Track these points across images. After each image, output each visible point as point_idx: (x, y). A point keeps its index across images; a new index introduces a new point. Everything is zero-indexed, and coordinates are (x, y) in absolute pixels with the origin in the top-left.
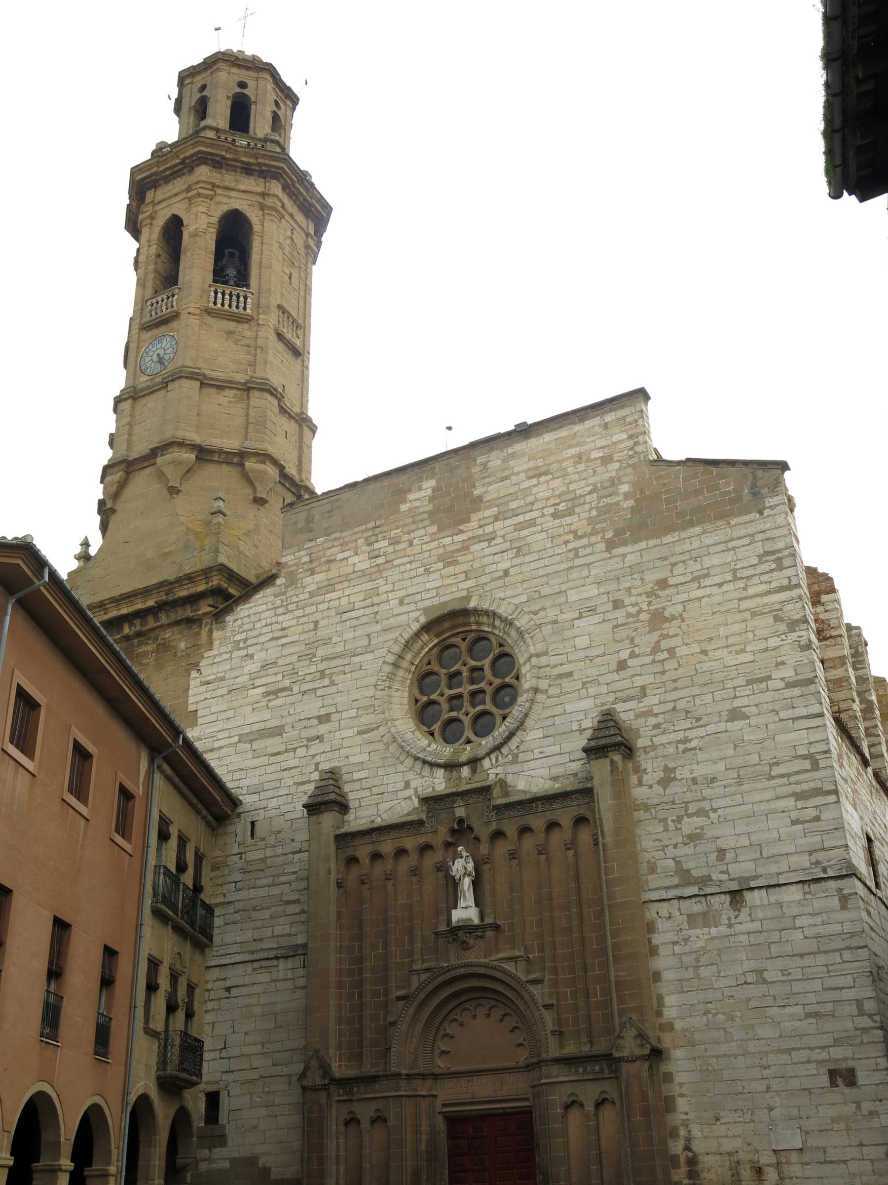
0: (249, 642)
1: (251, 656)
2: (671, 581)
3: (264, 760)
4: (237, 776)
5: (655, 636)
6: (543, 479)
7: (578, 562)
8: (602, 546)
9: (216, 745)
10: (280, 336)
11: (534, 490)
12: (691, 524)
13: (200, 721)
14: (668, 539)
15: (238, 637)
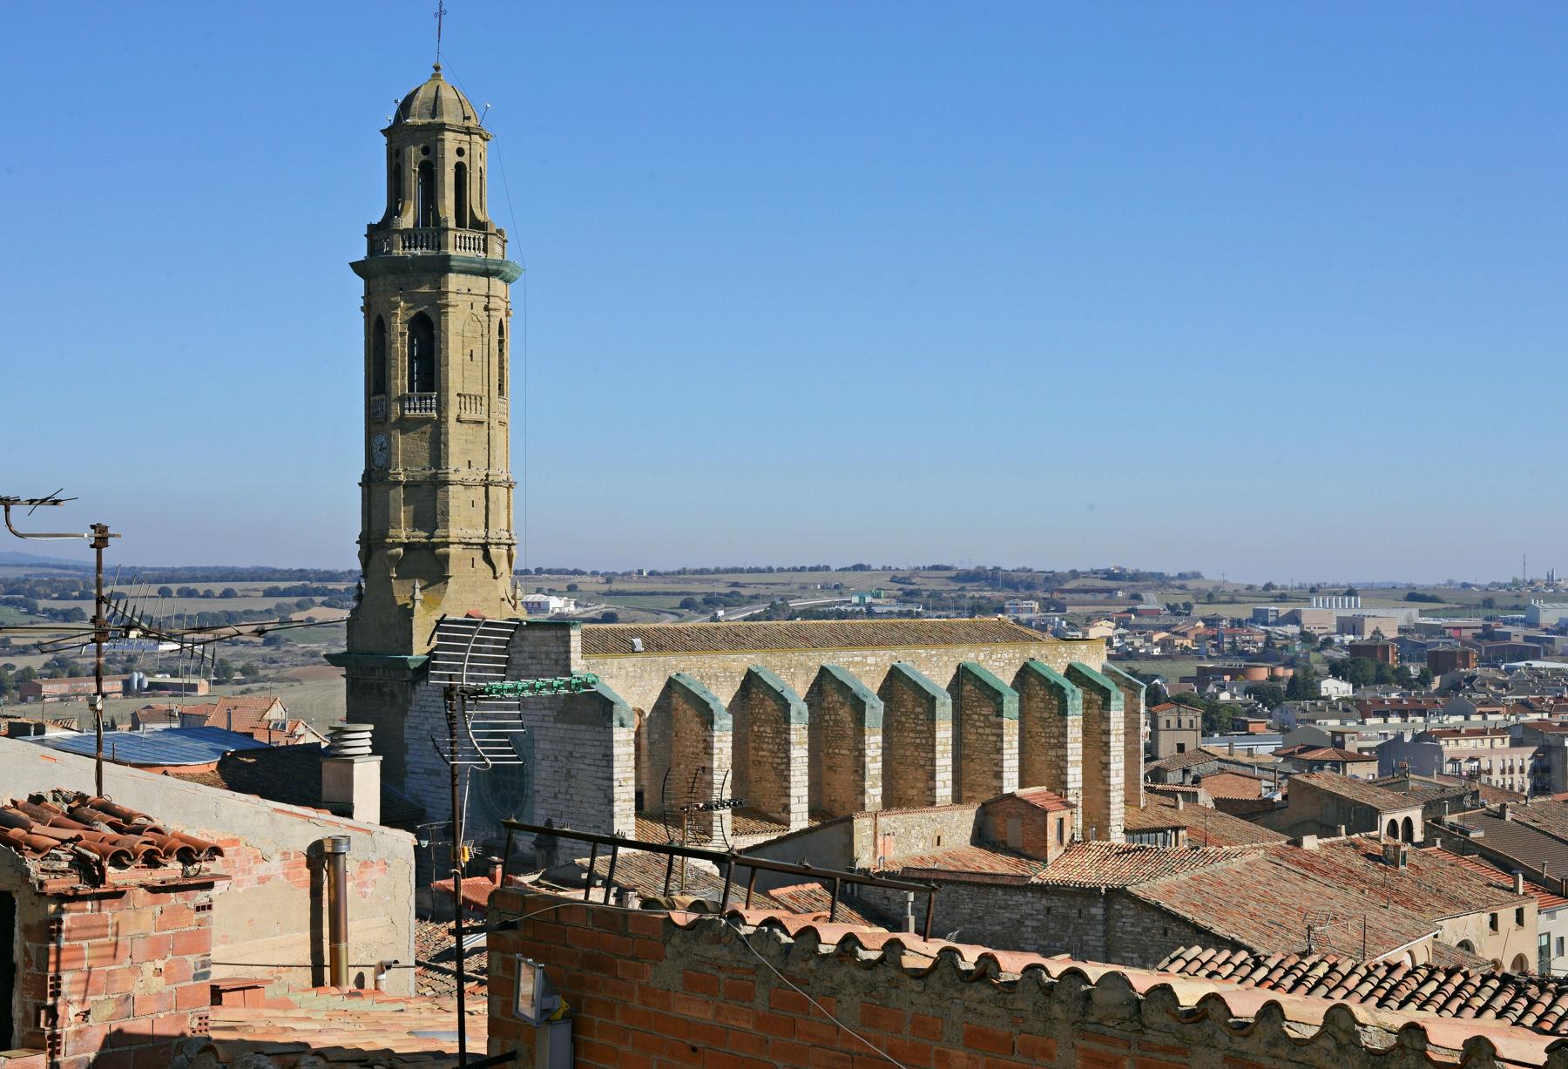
0: (427, 709)
1: (427, 718)
2: (575, 754)
3: (433, 789)
4: (425, 793)
5: (567, 784)
6: (534, 661)
7: (544, 724)
8: (552, 719)
9: (417, 770)
10: (458, 420)
11: (531, 667)
12: (581, 723)
13: (410, 752)
14: (575, 727)
15: (422, 703)
